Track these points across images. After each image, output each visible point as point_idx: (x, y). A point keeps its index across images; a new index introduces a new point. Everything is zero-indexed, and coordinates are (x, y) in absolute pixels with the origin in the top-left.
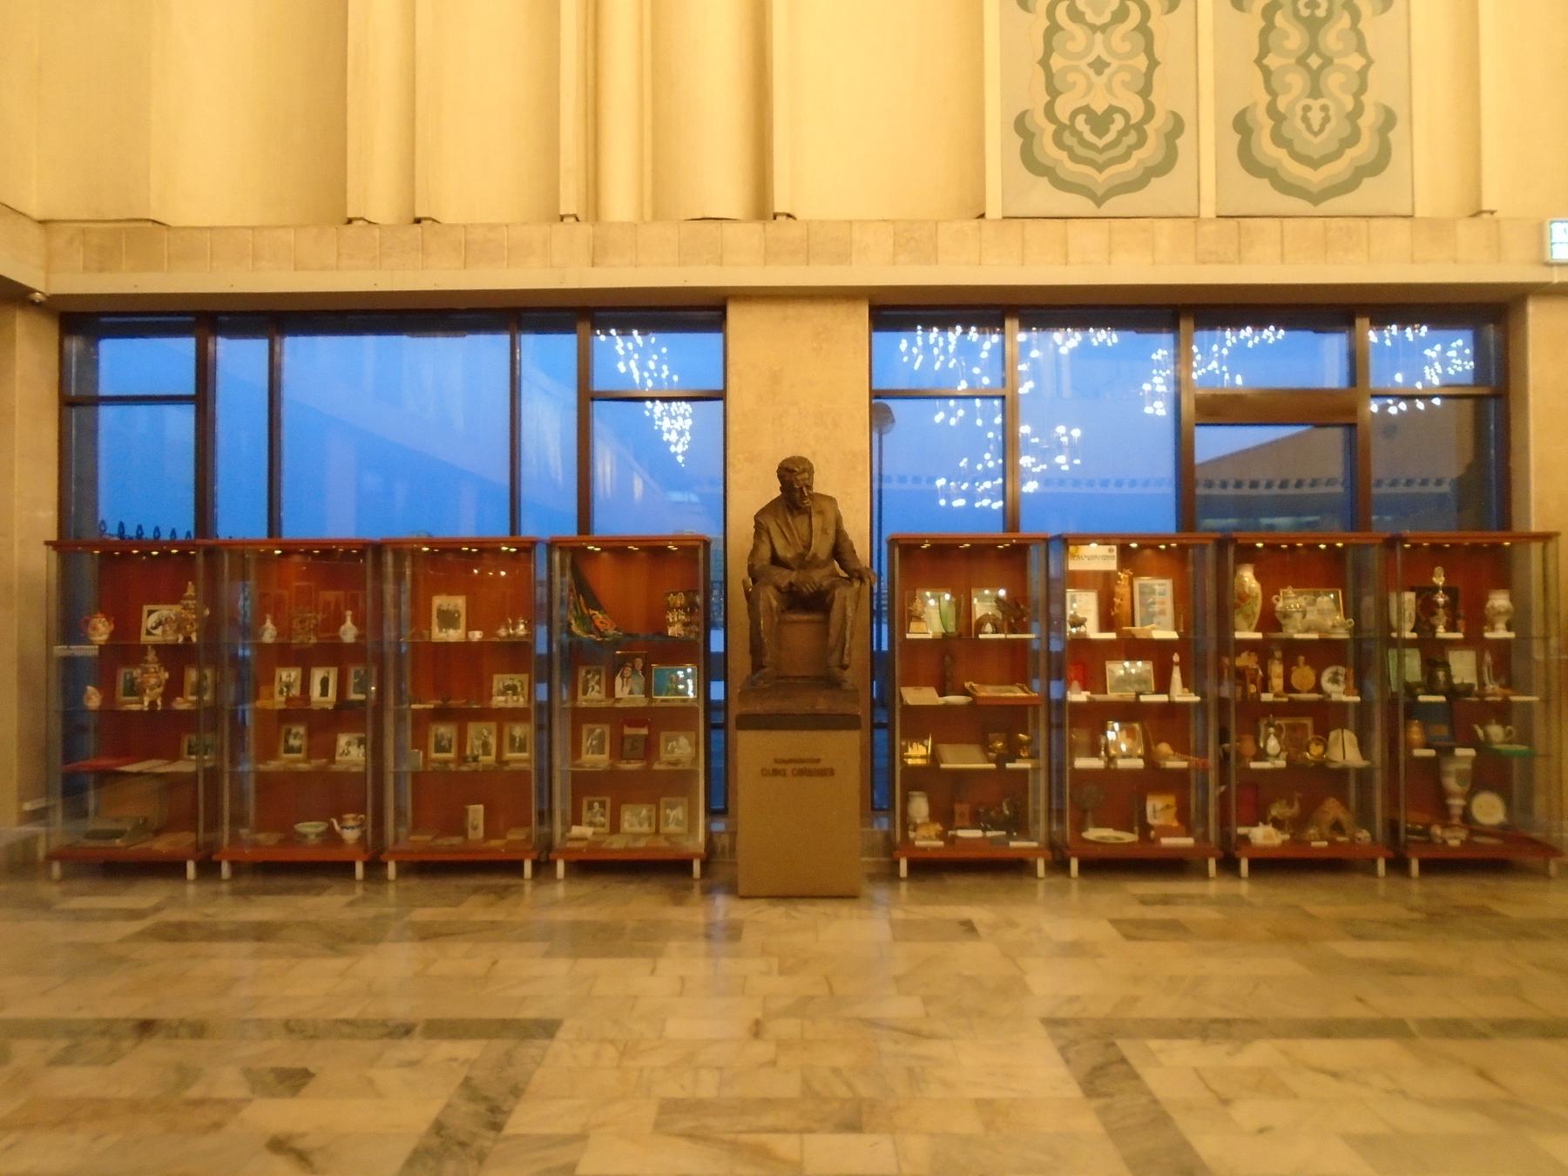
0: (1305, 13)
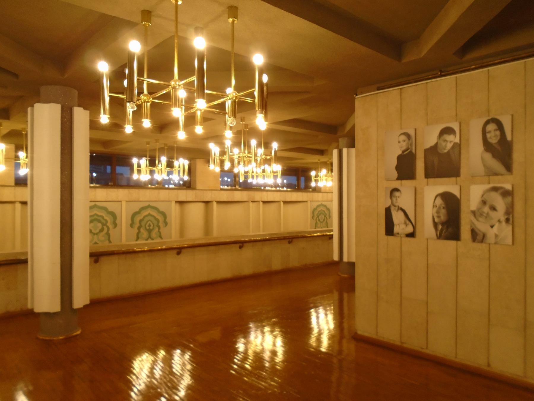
0: (148, 228)
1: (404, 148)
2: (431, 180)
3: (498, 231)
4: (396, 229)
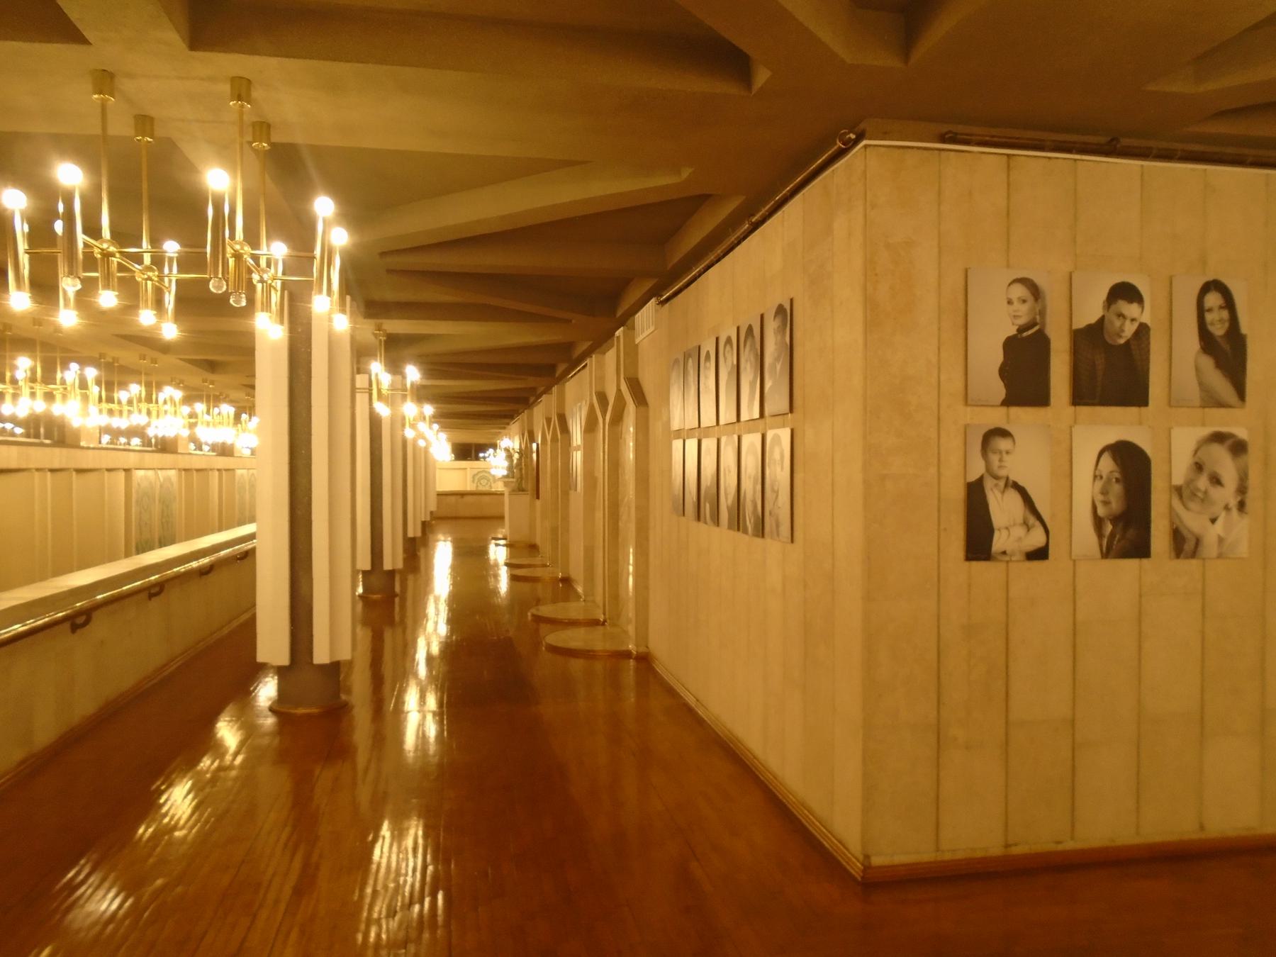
1: (1022, 321)
2: (1084, 410)
3: (1222, 529)
4: (999, 542)
